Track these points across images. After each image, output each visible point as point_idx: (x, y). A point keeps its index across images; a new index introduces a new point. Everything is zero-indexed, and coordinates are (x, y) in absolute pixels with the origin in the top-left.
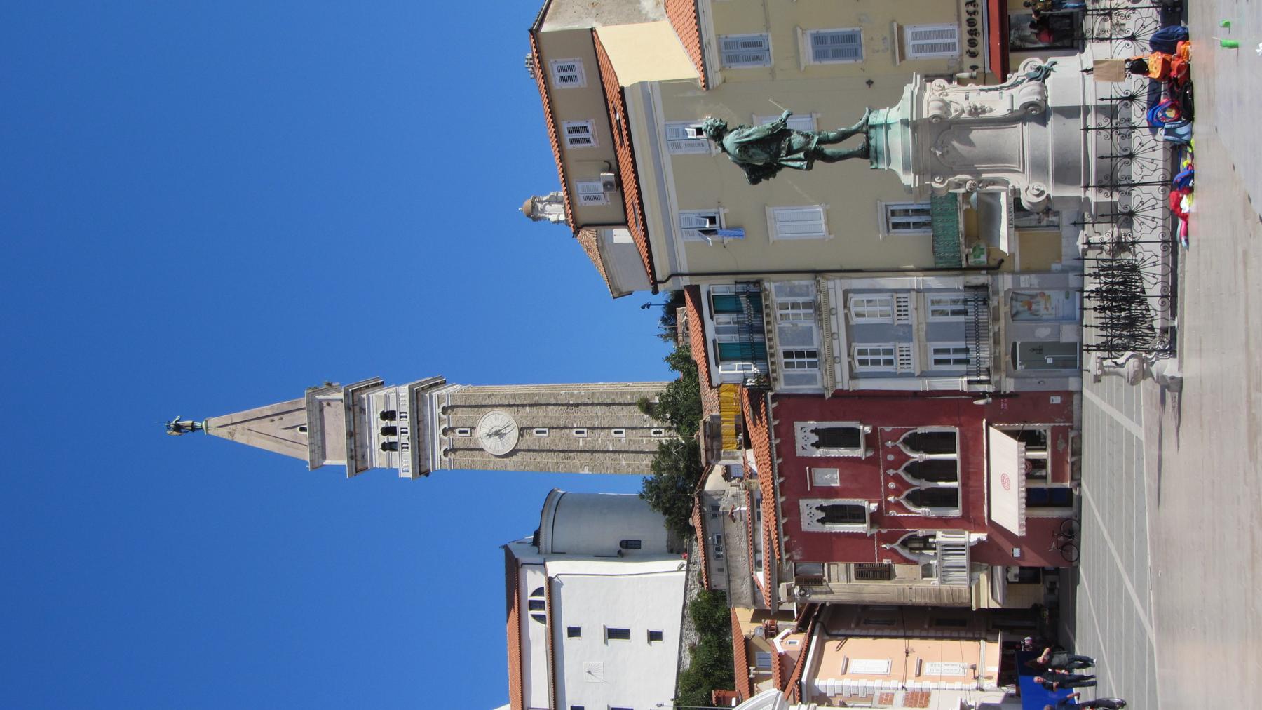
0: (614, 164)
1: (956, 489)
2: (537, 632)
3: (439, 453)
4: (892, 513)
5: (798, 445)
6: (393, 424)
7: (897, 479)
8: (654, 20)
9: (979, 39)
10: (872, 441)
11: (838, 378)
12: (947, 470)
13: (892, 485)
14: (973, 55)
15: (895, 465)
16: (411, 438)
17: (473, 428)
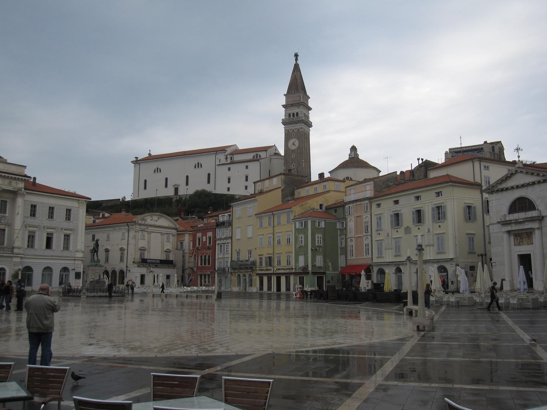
0: (263, 191)
1: (202, 265)
2: (250, 156)
3: (288, 129)
4: (199, 252)
5: (209, 233)
6: (295, 116)
7: (204, 253)
8: (282, 201)
9: (260, 271)
10: (209, 248)
11: (218, 241)
12: (205, 264)
13: (203, 252)
14: (259, 270)
15: (206, 252)
16: (291, 122)
17: (294, 137)
